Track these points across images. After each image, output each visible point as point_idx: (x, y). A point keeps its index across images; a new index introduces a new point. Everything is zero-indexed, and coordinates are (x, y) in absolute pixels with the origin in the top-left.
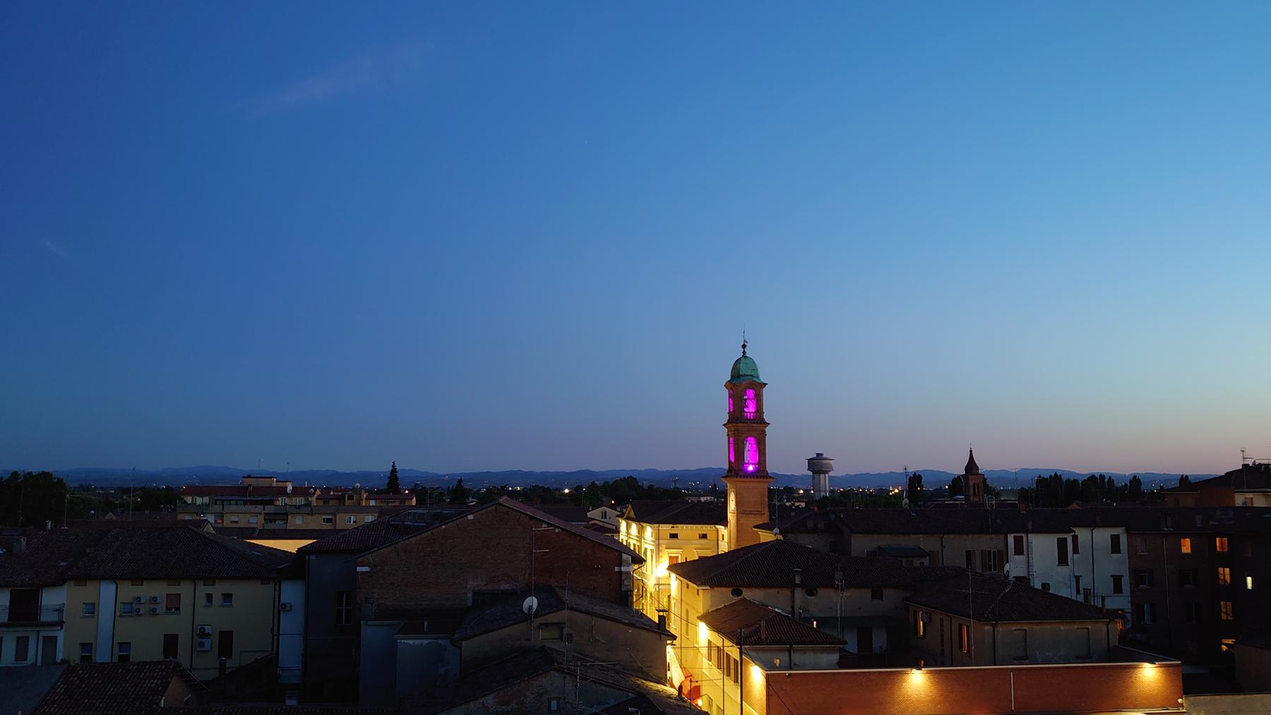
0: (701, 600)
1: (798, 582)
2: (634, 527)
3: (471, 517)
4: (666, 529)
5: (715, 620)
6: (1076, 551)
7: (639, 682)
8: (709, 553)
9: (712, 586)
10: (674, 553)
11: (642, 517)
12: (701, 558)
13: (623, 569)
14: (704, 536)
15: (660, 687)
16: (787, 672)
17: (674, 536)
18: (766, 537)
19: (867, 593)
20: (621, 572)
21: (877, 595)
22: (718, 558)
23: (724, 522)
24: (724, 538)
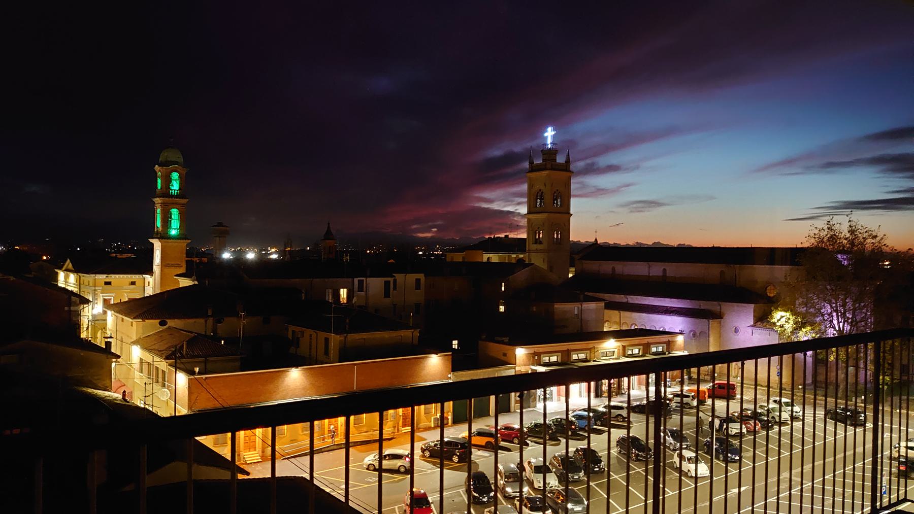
0: (134, 327)
1: (210, 314)
2: (72, 278)
5: (145, 343)
6: (395, 288)
7: (90, 390)
9: (144, 320)
11: (80, 268)
13: (72, 308)
15: (107, 393)
16: (204, 376)
18: (185, 282)
20: (70, 311)
22: (145, 298)
23: (150, 272)
24: (151, 285)
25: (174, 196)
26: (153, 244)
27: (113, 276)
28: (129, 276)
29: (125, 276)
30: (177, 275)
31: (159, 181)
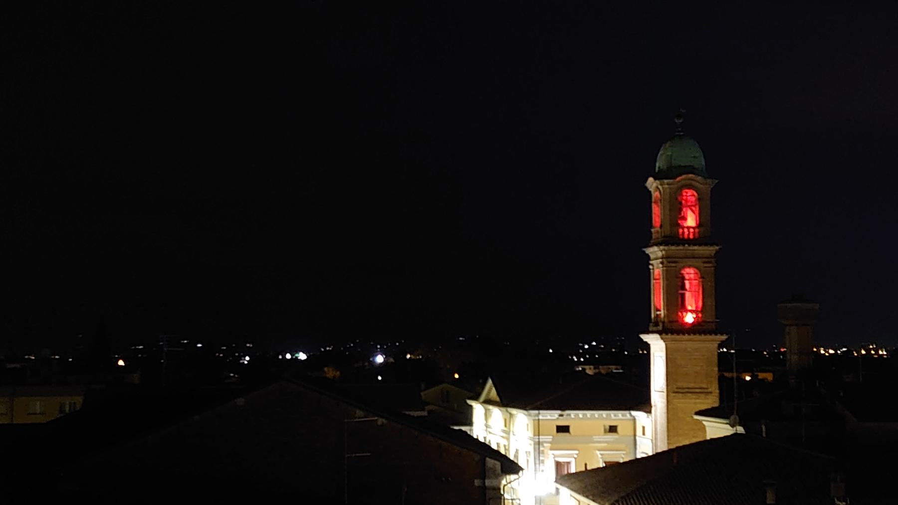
2: (497, 413)
4: (551, 417)
8: (623, 457)
10: (564, 456)
11: (509, 399)
12: (612, 467)
14: (613, 429)
17: (563, 429)
18: (717, 429)
22: (637, 461)
23: (643, 403)
25: (689, 242)
26: (647, 346)
27: (573, 413)
28: (604, 413)
29: (596, 413)
30: (699, 413)
31: (656, 210)
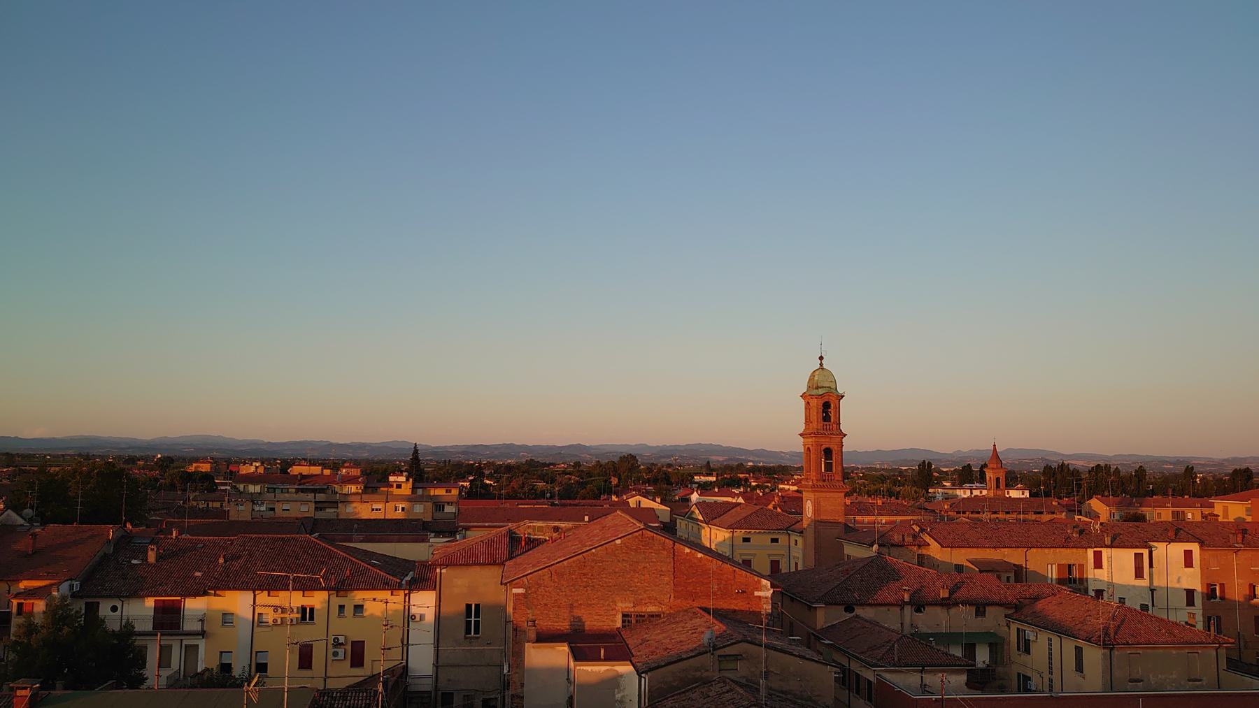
3: (618, 542)
19: (973, 609)
21: (980, 612)
